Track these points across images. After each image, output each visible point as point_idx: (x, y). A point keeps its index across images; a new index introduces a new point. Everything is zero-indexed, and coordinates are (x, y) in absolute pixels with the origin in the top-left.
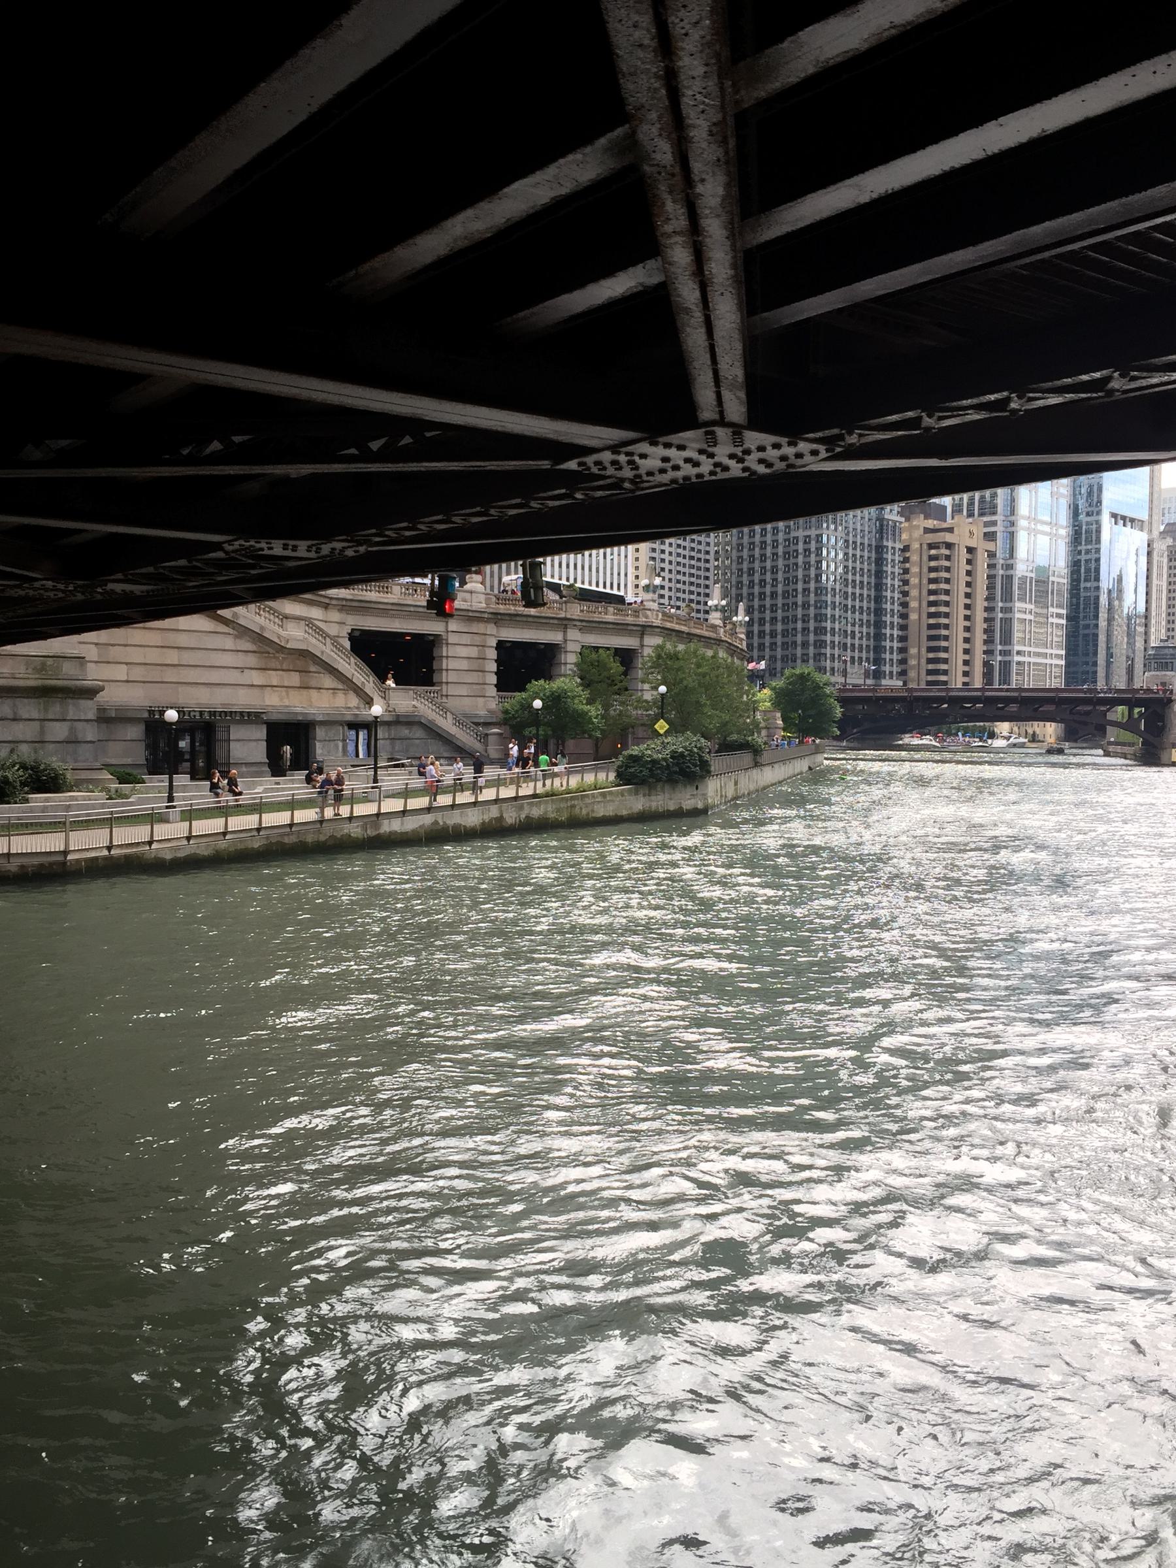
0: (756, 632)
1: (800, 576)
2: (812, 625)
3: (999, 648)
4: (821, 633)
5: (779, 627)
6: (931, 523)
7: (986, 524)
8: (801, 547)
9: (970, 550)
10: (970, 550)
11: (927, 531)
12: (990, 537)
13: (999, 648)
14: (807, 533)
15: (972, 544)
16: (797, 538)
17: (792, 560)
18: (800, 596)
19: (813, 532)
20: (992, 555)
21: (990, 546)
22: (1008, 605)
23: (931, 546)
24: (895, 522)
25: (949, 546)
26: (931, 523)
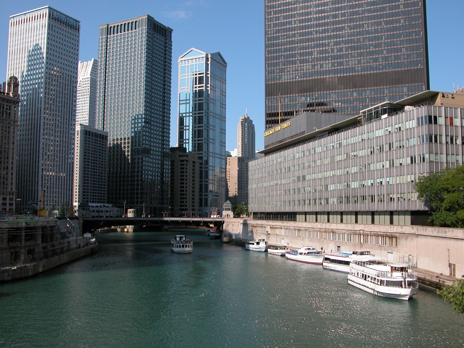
0: (122, 189)
1: (136, 171)
2: (140, 187)
3: (204, 194)
4: (142, 190)
5: (129, 188)
6: (181, 153)
7: (199, 154)
8: (136, 161)
9: (194, 162)
10: (194, 162)
11: (180, 156)
12: (201, 158)
13: (204, 194)
14: (138, 157)
15: (194, 160)
16: (135, 158)
17: (133, 165)
18: (136, 177)
19: (140, 157)
20: (201, 164)
21: (201, 161)
22: (207, 180)
23: (181, 161)
24: (168, 153)
25: (187, 161)
26: (181, 153)
